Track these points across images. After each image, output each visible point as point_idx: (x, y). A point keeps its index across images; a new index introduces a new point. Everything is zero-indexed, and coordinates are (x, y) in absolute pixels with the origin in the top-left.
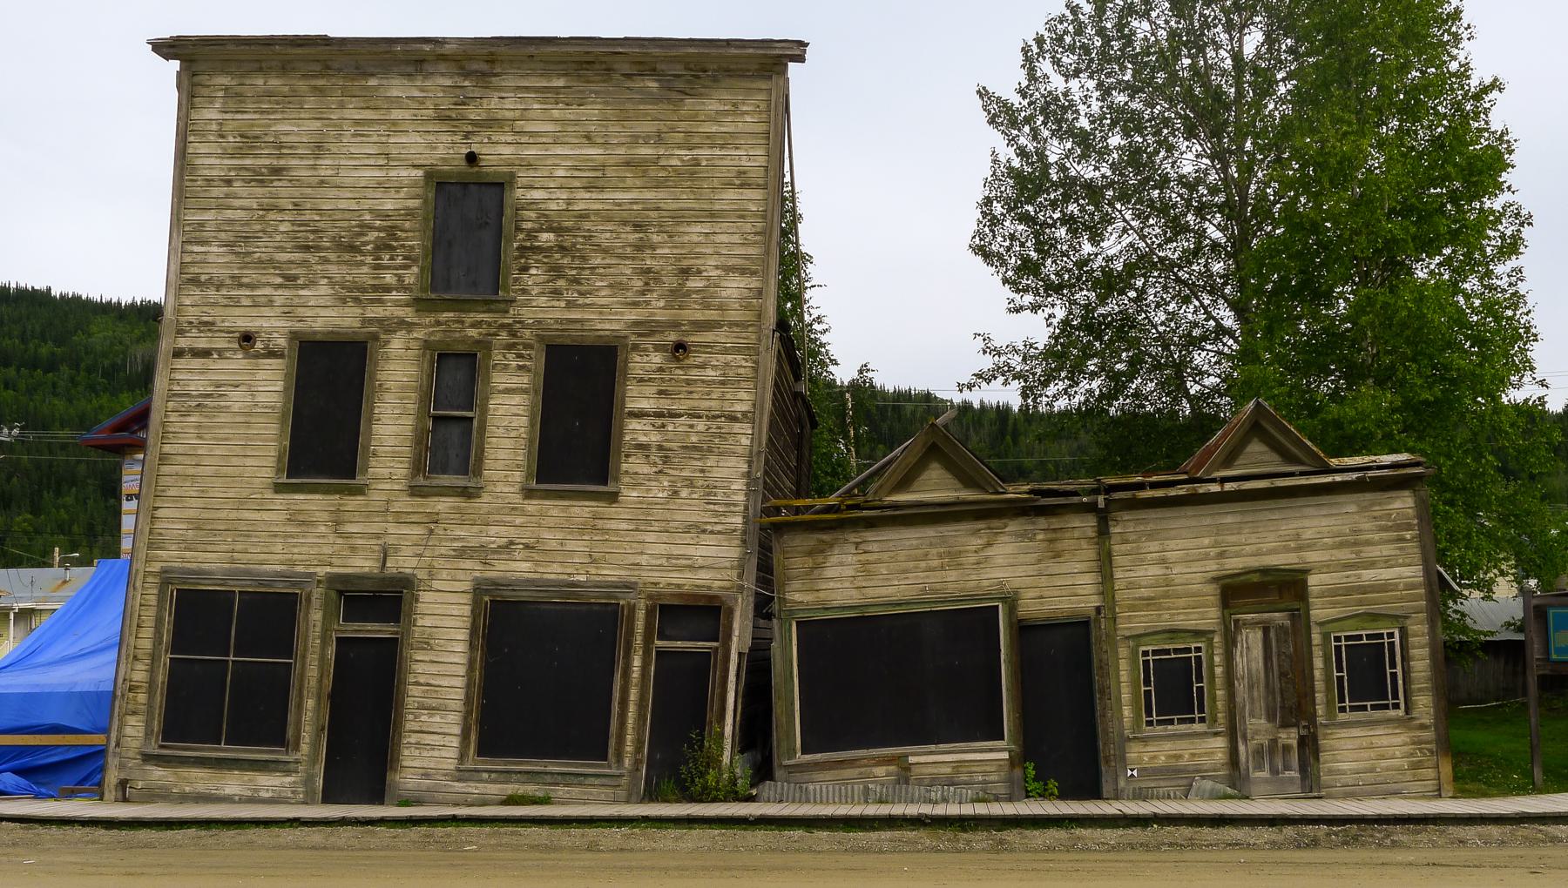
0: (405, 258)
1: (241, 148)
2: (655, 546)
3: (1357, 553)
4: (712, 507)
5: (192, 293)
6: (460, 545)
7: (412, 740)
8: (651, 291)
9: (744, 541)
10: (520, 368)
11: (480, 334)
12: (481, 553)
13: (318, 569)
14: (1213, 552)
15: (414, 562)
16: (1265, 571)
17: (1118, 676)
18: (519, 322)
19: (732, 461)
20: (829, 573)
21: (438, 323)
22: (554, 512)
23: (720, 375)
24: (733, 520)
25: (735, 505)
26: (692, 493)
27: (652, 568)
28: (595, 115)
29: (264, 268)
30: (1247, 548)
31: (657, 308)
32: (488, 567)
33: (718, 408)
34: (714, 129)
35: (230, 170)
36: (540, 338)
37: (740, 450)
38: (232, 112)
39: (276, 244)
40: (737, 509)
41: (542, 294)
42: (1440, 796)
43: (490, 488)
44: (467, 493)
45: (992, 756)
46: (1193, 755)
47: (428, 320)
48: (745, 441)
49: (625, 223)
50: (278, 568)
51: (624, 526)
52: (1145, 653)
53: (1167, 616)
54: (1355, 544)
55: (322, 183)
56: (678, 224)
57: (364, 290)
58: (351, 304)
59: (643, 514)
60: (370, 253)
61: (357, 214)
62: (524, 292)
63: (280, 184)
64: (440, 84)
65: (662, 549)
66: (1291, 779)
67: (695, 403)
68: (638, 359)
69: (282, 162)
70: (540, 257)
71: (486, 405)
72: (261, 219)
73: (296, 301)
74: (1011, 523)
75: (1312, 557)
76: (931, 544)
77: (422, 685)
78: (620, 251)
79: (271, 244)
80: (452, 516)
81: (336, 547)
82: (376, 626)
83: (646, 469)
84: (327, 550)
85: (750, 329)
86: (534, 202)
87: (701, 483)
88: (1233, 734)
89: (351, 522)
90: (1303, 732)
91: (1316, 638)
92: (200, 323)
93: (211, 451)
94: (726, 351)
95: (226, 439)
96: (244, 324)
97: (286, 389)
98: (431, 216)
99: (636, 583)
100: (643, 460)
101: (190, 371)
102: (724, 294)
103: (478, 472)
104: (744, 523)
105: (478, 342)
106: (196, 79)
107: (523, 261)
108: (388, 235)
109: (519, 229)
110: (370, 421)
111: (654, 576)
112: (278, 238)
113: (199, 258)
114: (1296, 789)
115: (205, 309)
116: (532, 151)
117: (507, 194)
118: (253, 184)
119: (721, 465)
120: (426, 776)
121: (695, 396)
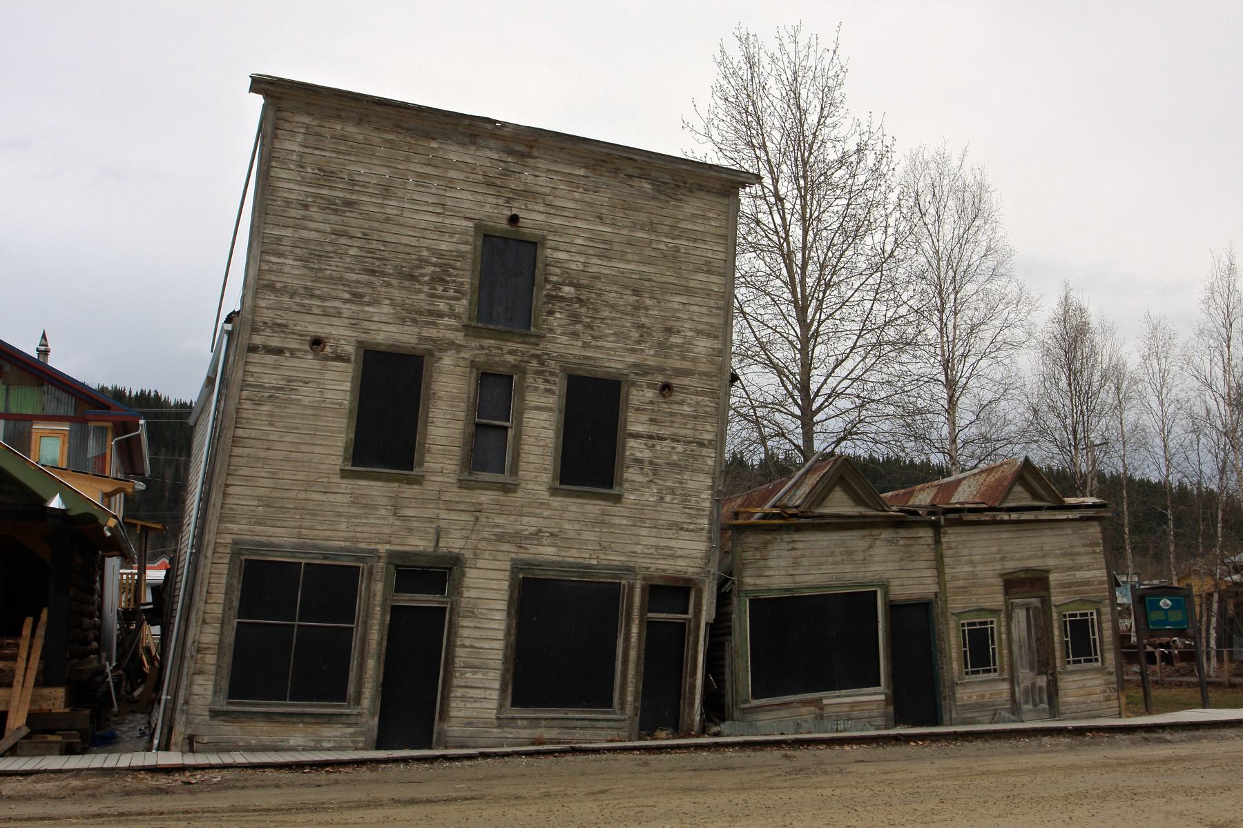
0: (456, 291)
1: (318, 179)
2: (648, 538)
4: (687, 510)
5: (268, 297)
6: (500, 530)
7: (458, 694)
8: (645, 342)
9: (710, 538)
10: (547, 390)
11: (516, 360)
12: (516, 538)
13: (379, 547)
14: (998, 557)
15: (460, 543)
16: (1027, 570)
17: (949, 641)
18: (547, 354)
19: (702, 477)
20: (771, 563)
21: (482, 348)
22: (573, 508)
23: (693, 411)
24: (702, 521)
25: (703, 510)
26: (673, 499)
27: (645, 555)
28: (605, 202)
29: (334, 284)
30: (1016, 555)
31: (649, 356)
32: (521, 550)
33: (692, 435)
34: (690, 227)
35: (307, 196)
36: (563, 369)
37: (706, 468)
38: (312, 148)
39: (346, 265)
40: (705, 513)
41: (564, 334)
42: (1120, 717)
44: (507, 489)
45: (874, 697)
46: (991, 694)
47: (473, 344)
48: (710, 462)
49: (626, 287)
50: (343, 544)
51: (625, 522)
52: (963, 625)
53: (975, 600)
54: (1072, 554)
55: (388, 220)
56: (665, 293)
57: (421, 313)
58: (409, 323)
60: (428, 284)
61: (417, 249)
62: (551, 331)
63: (352, 215)
64: (486, 157)
65: (652, 541)
66: (1044, 709)
67: (676, 431)
68: (635, 392)
69: (354, 197)
70: (563, 305)
71: (522, 417)
72: (333, 243)
73: (362, 316)
74: (884, 532)
75: (1051, 562)
76: (835, 545)
77: (466, 647)
78: (623, 308)
79: (341, 265)
80: (493, 507)
82: (430, 597)
83: (640, 478)
84: (386, 530)
85: (714, 379)
86: (559, 261)
88: (1012, 680)
89: (408, 507)
90: (1051, 678)
91: (1055, 616)
92: (274, 324)
93: (282, 437)
94: (697, 393)
95: (297, 428)
96: (315, 329)
97: (353, 390)
98: (479, 260)
99: (634, 567)
101: (264, 365)
102: (696, 350)
103: (515, 470)
104: (710, 524)
105: (515, 366)
106: (281, 114)
107: (550, 306)
108: (442, 270)
109: (547, 281)
110: (426, 423)
111: (646, 562)
112: (348, 260)
113: (275, 267)
114: (1046, 715)
115: (279, 312)
116: (558, 221)
117: (539, 252)
118: (327, 211)
119: (694, 479)
120: (470, 724)
121: (676, 425)
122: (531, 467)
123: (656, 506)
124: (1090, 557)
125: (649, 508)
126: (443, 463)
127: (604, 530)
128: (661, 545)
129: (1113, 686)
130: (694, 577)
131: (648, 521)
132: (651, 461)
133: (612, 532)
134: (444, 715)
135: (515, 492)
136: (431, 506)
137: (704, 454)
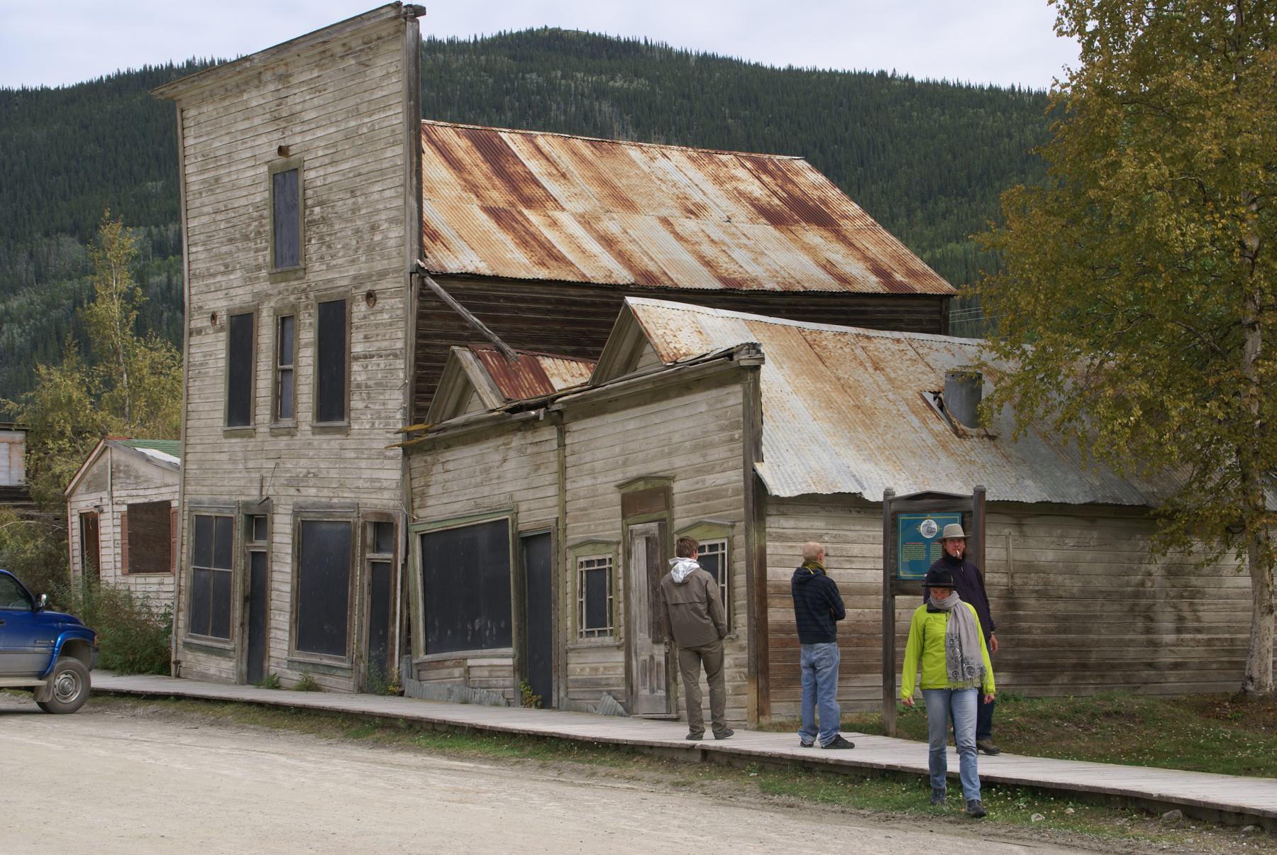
3: (704, 456)
46: (605, 668)
65: (367, 474)
75: (679, 462)
87: (383, 415)
124: (726, 448)
129: (742, 669)
130: (391, 511)
131: (366, 452)
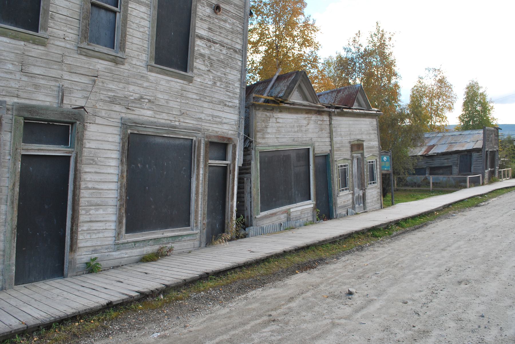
4: (228, 93)
6: (113, 94)
13: (7, 99)
14: (349, 133)
26: (221, 84)
32: (129, 111)
33: (230, 44)
37: (238, 67)
43: (129, 60)
45: (309, 205)
51: (195, 97)
59: (203, 92)
65: (209, 112)
67: (222, 39)
68: (200, 7)
71: (127, 6)
74: (313, 116)
75: (364, 137)
77: (90, 189)
80: (107, 74)
81: (21, 83)
83: (203, 68)
87: (224, 80)
89: (35, 65)
100: (202, 63)
103: (123, 48)
119: (231, 73)
121: (222, 35)
122: (134, 47)
123: (212, 88)
125: (208, 89)
126: (65, 31)
127: (183, 101)
128: (215, 114)
131: (208, 98)
132: (209, 57)
133: (187, 103)
134: (73, 247)
135: (123, 64)
136: (55, 67)
137: (236, 57)
